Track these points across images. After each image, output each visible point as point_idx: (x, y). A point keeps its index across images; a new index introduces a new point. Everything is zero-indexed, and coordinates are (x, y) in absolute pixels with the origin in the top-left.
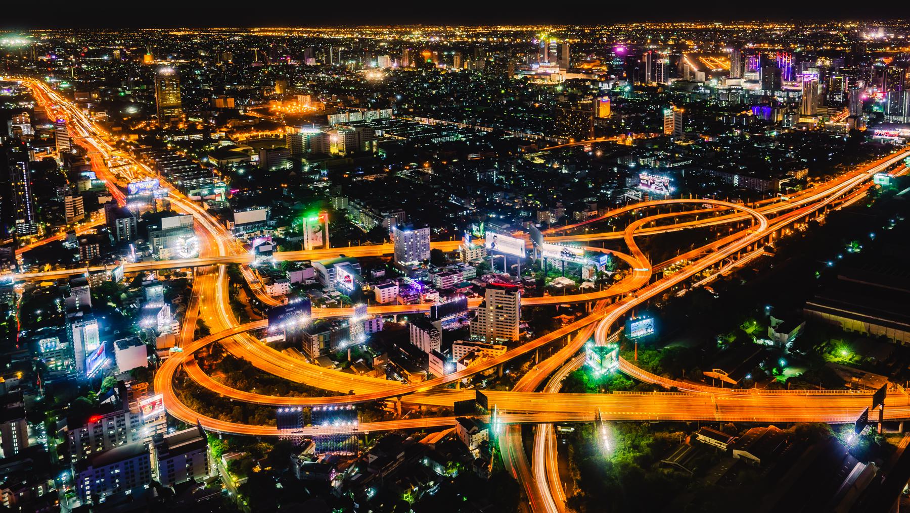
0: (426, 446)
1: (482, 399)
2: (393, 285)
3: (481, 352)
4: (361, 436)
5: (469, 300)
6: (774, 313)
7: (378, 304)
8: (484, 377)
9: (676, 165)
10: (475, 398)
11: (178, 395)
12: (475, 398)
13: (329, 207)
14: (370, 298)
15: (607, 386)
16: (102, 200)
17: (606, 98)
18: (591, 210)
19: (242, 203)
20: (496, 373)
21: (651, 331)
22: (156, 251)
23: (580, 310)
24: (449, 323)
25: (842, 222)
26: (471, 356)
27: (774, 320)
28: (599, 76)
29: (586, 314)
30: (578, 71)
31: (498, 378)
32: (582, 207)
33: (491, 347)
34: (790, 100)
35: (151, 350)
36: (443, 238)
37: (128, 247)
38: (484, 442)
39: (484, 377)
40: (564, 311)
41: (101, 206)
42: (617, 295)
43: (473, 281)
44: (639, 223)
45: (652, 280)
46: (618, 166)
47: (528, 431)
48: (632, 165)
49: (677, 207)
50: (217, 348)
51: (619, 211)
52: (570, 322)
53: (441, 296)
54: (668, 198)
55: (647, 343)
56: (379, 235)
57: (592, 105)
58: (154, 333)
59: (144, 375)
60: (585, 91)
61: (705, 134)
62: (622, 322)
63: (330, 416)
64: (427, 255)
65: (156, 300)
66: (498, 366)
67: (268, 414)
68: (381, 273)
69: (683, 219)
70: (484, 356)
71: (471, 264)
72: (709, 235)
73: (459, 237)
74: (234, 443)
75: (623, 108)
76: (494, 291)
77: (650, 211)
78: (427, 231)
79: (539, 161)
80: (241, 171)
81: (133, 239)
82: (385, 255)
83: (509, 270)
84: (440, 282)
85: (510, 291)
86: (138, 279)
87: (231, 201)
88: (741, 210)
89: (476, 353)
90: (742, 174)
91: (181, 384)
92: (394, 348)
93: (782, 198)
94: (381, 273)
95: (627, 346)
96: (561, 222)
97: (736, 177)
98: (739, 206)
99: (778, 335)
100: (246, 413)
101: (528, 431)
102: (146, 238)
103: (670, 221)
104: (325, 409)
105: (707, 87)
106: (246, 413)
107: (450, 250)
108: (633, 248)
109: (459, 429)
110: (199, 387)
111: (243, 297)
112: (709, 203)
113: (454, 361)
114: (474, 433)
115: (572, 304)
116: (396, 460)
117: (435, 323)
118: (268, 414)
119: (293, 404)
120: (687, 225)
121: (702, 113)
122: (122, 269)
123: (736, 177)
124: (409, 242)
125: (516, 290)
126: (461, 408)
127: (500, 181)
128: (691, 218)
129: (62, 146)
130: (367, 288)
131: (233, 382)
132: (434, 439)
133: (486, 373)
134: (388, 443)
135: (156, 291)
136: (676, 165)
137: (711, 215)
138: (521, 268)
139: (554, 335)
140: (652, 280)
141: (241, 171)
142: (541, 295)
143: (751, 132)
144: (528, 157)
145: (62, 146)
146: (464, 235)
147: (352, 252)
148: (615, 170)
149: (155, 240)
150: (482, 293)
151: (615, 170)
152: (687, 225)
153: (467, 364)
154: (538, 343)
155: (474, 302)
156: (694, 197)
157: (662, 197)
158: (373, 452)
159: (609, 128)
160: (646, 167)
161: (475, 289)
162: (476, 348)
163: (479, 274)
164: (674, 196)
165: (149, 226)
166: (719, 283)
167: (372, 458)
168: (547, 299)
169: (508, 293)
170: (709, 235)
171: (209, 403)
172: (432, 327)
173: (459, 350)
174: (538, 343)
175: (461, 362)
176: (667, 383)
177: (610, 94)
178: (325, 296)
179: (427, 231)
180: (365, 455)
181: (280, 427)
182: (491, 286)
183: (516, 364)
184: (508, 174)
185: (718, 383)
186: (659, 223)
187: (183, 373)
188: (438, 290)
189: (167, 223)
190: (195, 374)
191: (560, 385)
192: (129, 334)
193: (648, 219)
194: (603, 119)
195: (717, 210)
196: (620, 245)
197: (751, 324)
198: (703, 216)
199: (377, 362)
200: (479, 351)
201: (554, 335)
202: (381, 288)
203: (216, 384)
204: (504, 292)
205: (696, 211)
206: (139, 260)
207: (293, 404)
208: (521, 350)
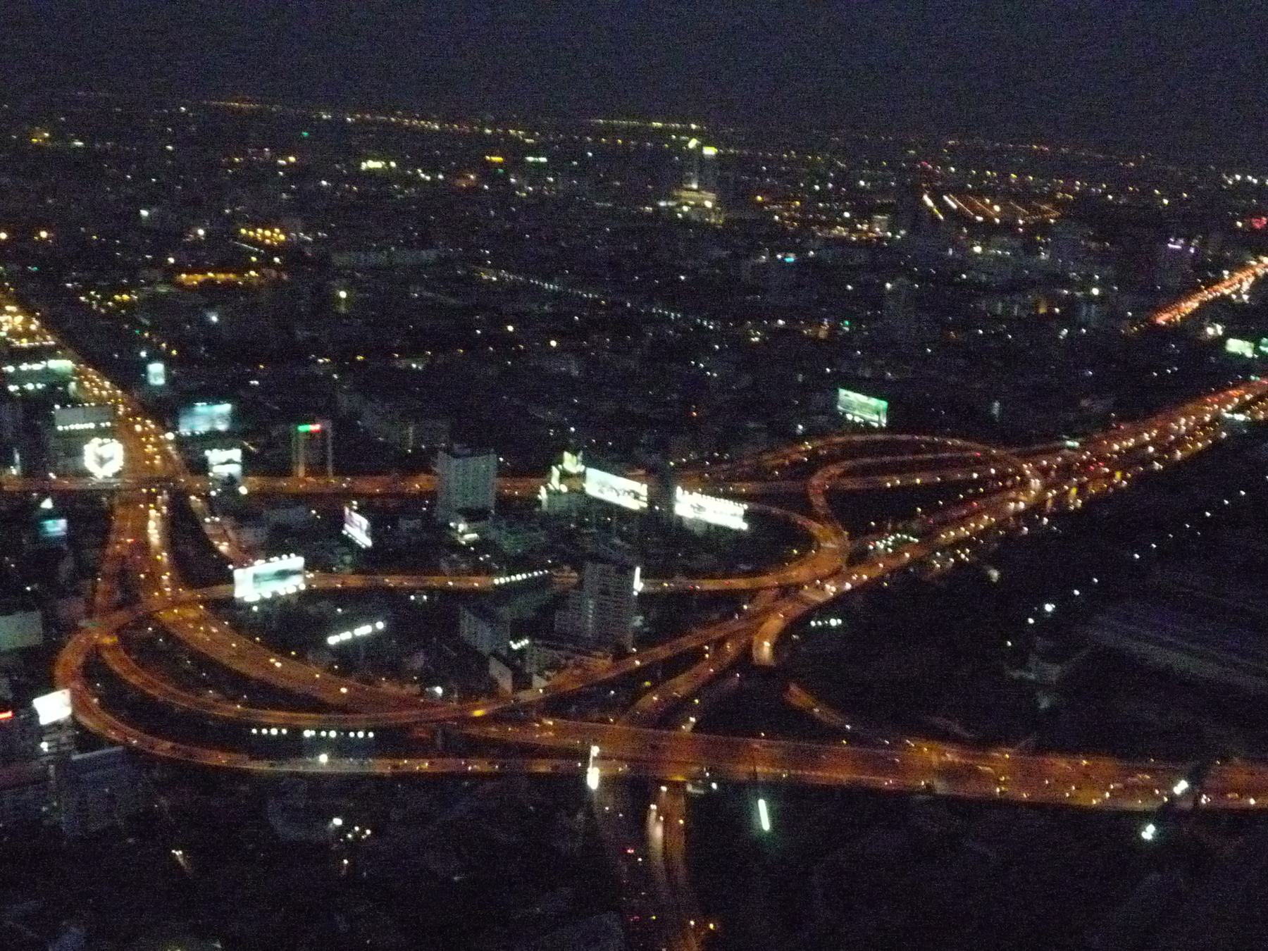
3: (571, 661)
26: (555, 666)
33: (589, 655)
42: (790, 585)
44: (834, 470)
70: (577, 666)
89: (563, 662)
93: (1069, 443)
123: (997, 404)
147: (373, 486)
150: (578, 567)
153: (548, 679)
154: (662, 652)
174: (662, 652)
175: (540, 674)
182: (596, 558)
183: (631, 684)
186: (866, 471)
200: (567, 658)
201: (688, 643)
204: (613, 569)
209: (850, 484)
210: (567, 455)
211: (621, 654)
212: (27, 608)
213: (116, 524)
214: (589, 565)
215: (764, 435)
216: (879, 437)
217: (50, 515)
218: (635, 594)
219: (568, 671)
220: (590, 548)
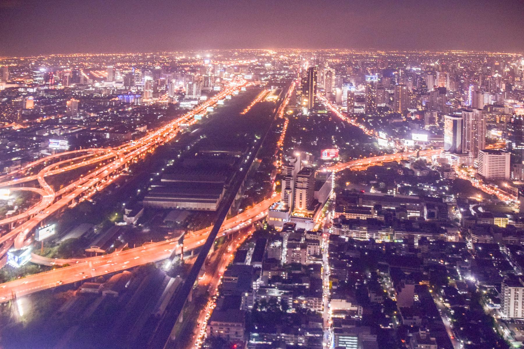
6: (127, 207)
9: (73, 131)
25: (162, 152)
28: (28, 85)
30: (14, 83)
49: (73, 156)
54: (67, 151)
57: (22, 102)
72: (93, 167)
75: (42, 102)
88: (110, 152)
90: (111, 132)
98: (109, 150)
99: (129, 218)
103: (68, 164)
112: (91, 151)
120: (79, 165)
136: (73, 131)
137: (93, 157)
143: (117, 110)
152: (79, 165)
157: (63, 151)
164: (70, 150)
170: (93, 167)
177: (33, 94)
185: (93, 254)
194: (28, 110)
195: (96, 154)
205: (84, 156)
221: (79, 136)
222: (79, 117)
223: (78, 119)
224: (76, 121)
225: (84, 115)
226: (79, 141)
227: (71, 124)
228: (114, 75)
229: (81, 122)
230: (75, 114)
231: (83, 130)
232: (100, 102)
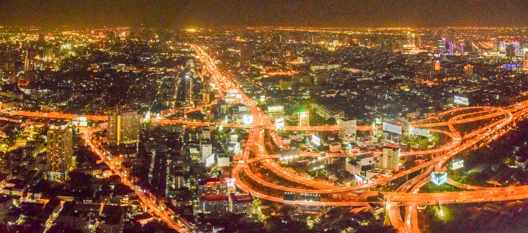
0: (353, 213)
1: (381, 196)
2: (338, 144)
4: (322, 207)
5: (375, 153)
7: (331, 152)
8: (381, 186)
10: (377, 195)
11: (241, 180)
12: (377, 195)
13: (309, 107)
14: (327, 149)
15: (440, 189)
16: (216, 96)
17: (438, 61)
18: (432, 113)
19: (271, 103)
20: (388, 184)
21: (462, 166)
22: (235, 119)
23: (428, 158)
24: (364, 162)
27: (517, 157)
29: (430, 159)
31: (388, 187)
32: (428, 111)
34: (518, 62)
35: (231, 160)
36: (363, 124)
37: (225, 117)
38: (381, 213)
39: (381, 186)
40: (420, 158)
41: (216, 98)
43: (376, 144)
45: (461, 144)
46: (445, 92)
47: (402, 210)
48: (451, 92)
50: (259, 164)
51: (445, 113)
52: (423, 163)
53: (361, 150)
55: (460, 172)
56: (332, 122)
58: (233, 153)
59: (228, 169)
60: (428, 58)
61: (483, 76)
62: (448, 162)
63: (308, 198)
64: (355, 132)
65: (234, 141)
66: (388, 182)
67: (280, 193)
68: (333, 139)
69: (475, 116)
70: (382, 177)
71: (375, 136)
73: (370, 124)
74: (265, 202)
76: (387, 149)
77: (461, 113)
78: (355, 121)
79: (407, 90)
80: (272, 89)
81: (227, 113)
82: (335, 131)
83: (393, 140)
84: (360, 144)
85: (395, 149)
86: (227, 131)
87: (267, 102)
91: (242, 176)
92: (338, 169)
94: (333, 139)
95: (451, 173)
96: (418, 118)
97: (498, 96)
100: (269, 191)
101: (402, 210)
102: (232, 114)
103: (469, 117)
104: (306, 195)
105: (482, 56)
106: (269, 191)
107: (366, 130)
108: (452, 129)
109: (369, 207)
110: (251, 179)
111: (270, 143)
113: (367, 179)
114: (377, 209)
115: (424, 155)
116: (338, 218)
117: (358, 162)
118: (280, 193)
119: (291, 190)
121: (482, 68)
122: (222, 125)
124: (347, 127)
125: (398, 149)
126: (370, 199)
127: (389, 99)
128: (478, 115)
129: (204, 73)
130: (326, 145)
131: (264, 178)
132: (357, 211)
133: (383, 185)
134: (334, 212)
135: (235, 137)
138: (399, 138)
139: (416, 169)
140: (461, 144)
141: (272, 89)
142: (409, 151)
144: (402, 88)
145: (204, 73)
146: (372, 123)
148: (443, 94)
149: (235, 115)
150: (381, 149)
151: (443, 94)
155: (377, 153)
156: (479, 106)
158: (328, 214)
159: (440, 76)
160: (457, 94)
161: (377, 147)
162: (378, 174)
163: (379, 141)
165: (234, 110)
166: (493, 143)
167: (327, 216)
168: (412, 153)
169: (394, 150)
171: (255, 185)
172: (357, 164)
173: (369, 174)
175: (371, 179)
176: (469, 187)
178: (307, 147)
179: (355, 121)
180: (324, 215)
181: (285, 199)
182: (386, 147)
184: (393, 96)
186: (464, 118)
187: (243, 172)
188: (359, 147)
189: (241, 109)
190: (249, 173)
191: (418, 190)
192: (223, 152)
193: (459, 116)
196: (447, 128)
197: (507, 160)
198: (484, 114)
199: (330, 177)
202: (332, 145)
203: (257, 178)
206: (229, 123)
207: (291, 190)
208: (400, 175)
209: (459, 122)
210: (377, 119)
211: (394, 173)
212: (226, 157)
213: (250, 137)
214: (384, 149)
215: (434, 110)
216: (467, 108)
217: (233, 134)
218: (399, 156)
219: (379, 179)
220: (385, 145)
221: (476, 95)
222: (474, 80)
223: (473, 82)
224: (472, 83)
225: (478, 79)
226: (476, 99)
227: (469, 85)
228: (498, 46)
229: (475, 84)
230: (471, 77)
231: (478, 91)
232: (489, 68)
